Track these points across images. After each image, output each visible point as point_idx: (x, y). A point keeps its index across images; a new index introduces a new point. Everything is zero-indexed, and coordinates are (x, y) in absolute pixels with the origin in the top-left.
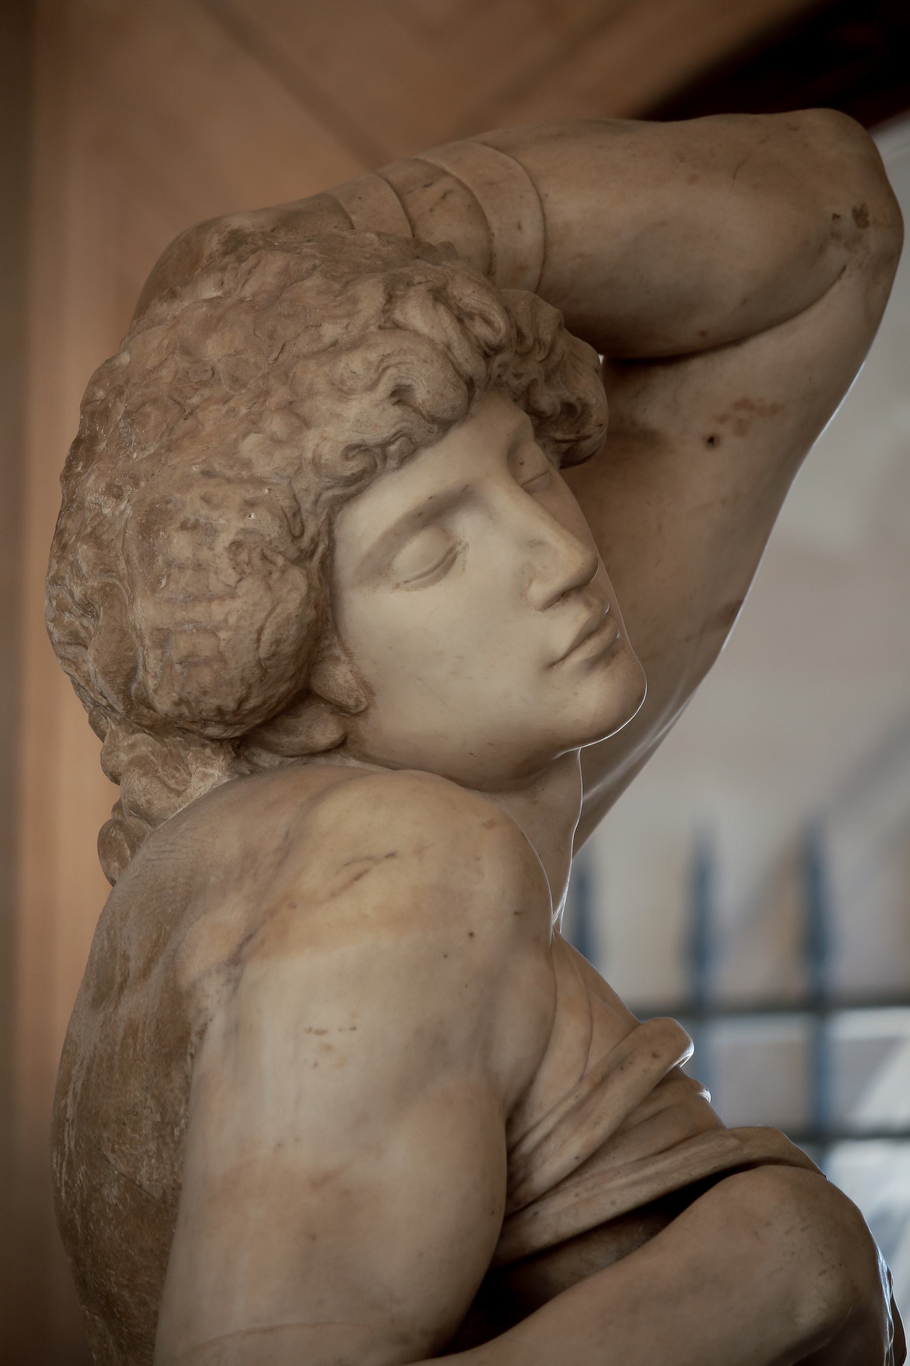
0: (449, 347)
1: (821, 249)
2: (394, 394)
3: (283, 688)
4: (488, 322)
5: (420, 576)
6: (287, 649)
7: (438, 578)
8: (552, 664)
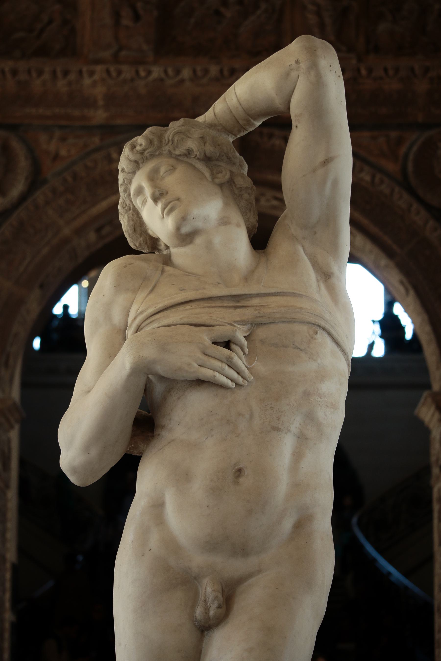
0: (128, 156)
1: (288, 74)
2: (122, 170)
3: (141, 239)
4: (141, 145)
5: (142, 207)
6: (130, 232)
7: (144, 207)
8: (163, 217)
